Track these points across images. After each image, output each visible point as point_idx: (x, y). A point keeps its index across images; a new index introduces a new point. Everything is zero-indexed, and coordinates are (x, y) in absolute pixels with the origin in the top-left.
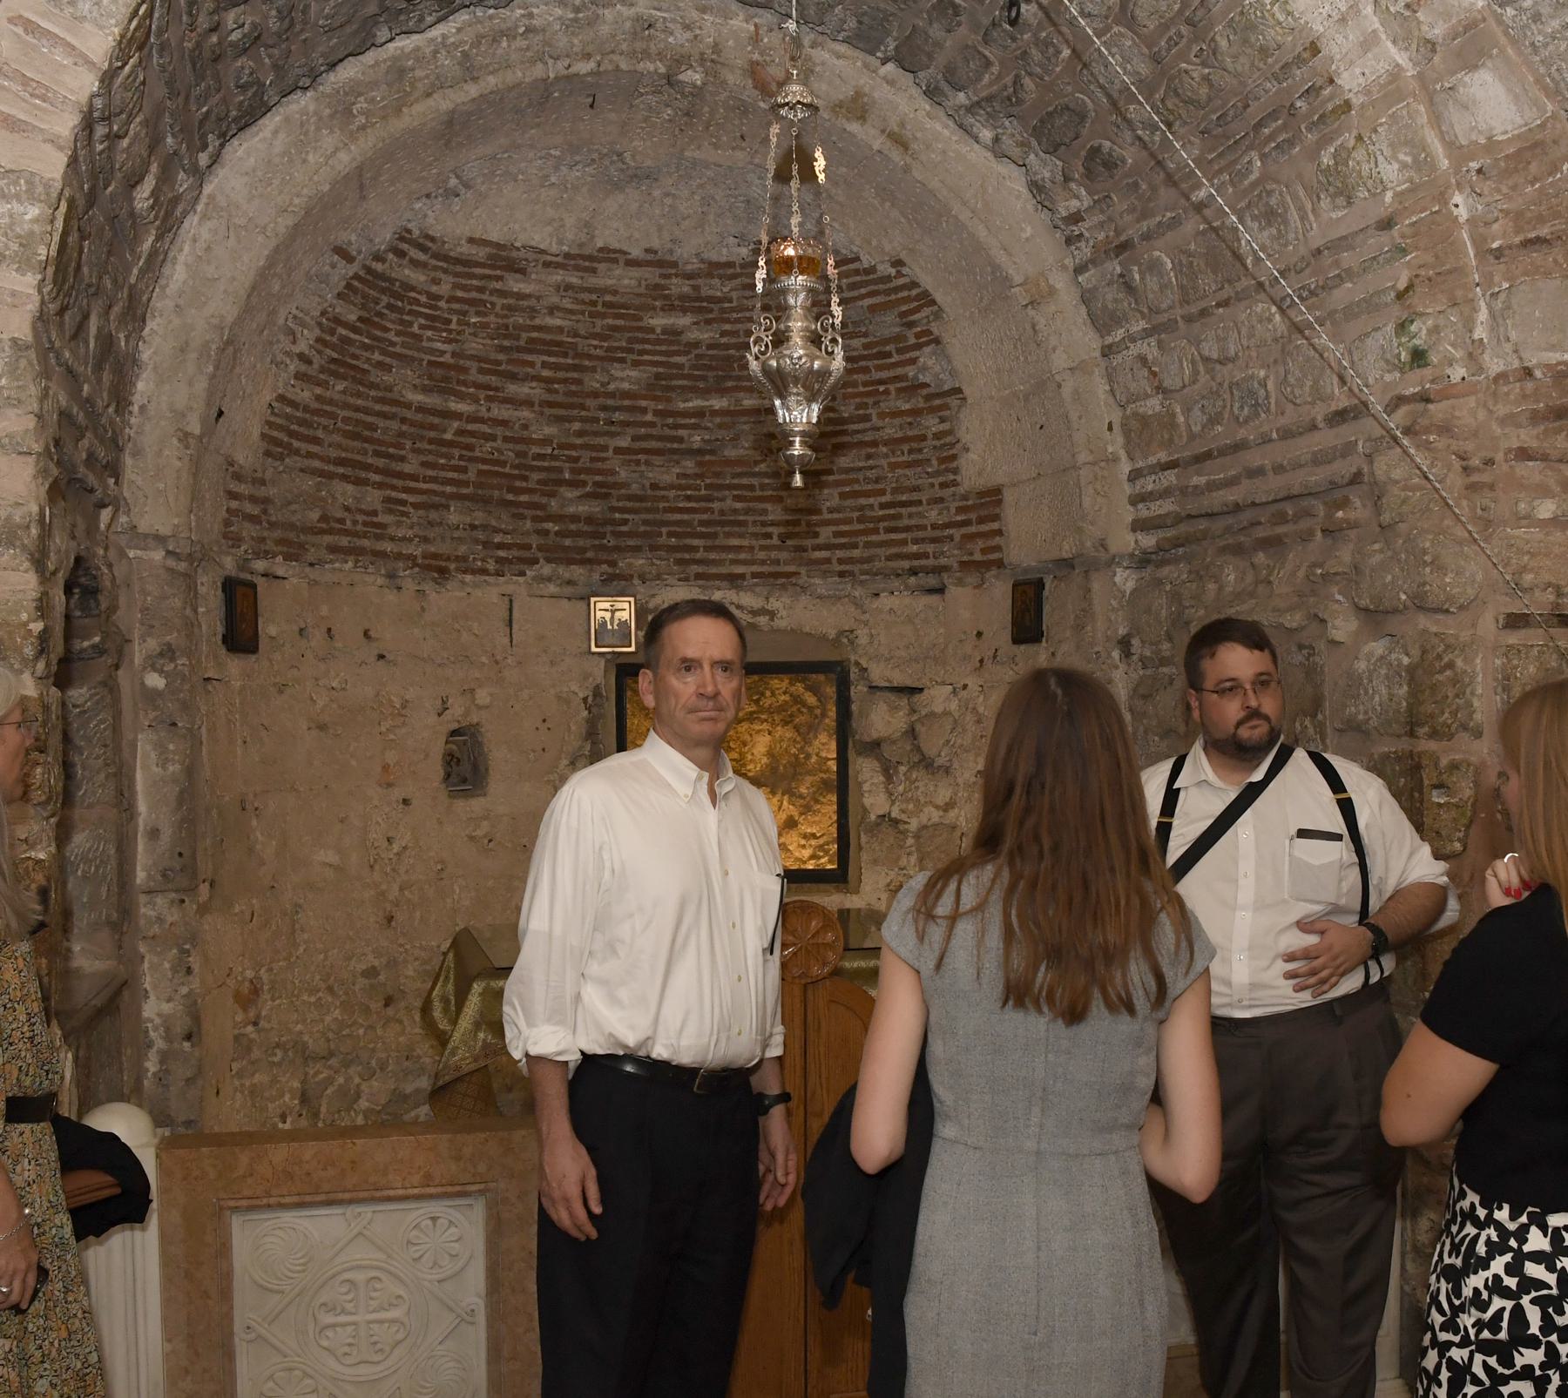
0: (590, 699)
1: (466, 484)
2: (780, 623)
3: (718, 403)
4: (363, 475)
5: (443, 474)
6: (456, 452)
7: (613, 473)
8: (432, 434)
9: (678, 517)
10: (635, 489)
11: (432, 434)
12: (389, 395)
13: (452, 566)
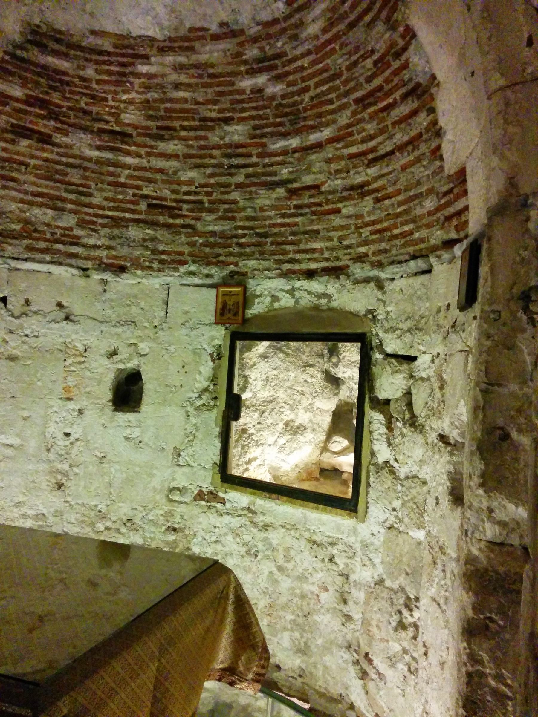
0: (215, 354)
1: (140, 212)
2: (334, 304)
3: (294, 142)
4: (60, 204)
5: (123, 205)
6: (131, 192)
7: (235, 202)
8: (111, 179)
9: (276, 230)
10: (249, 212)
11: (111, 179)
12: (70, 152)
13: (128, 265)
